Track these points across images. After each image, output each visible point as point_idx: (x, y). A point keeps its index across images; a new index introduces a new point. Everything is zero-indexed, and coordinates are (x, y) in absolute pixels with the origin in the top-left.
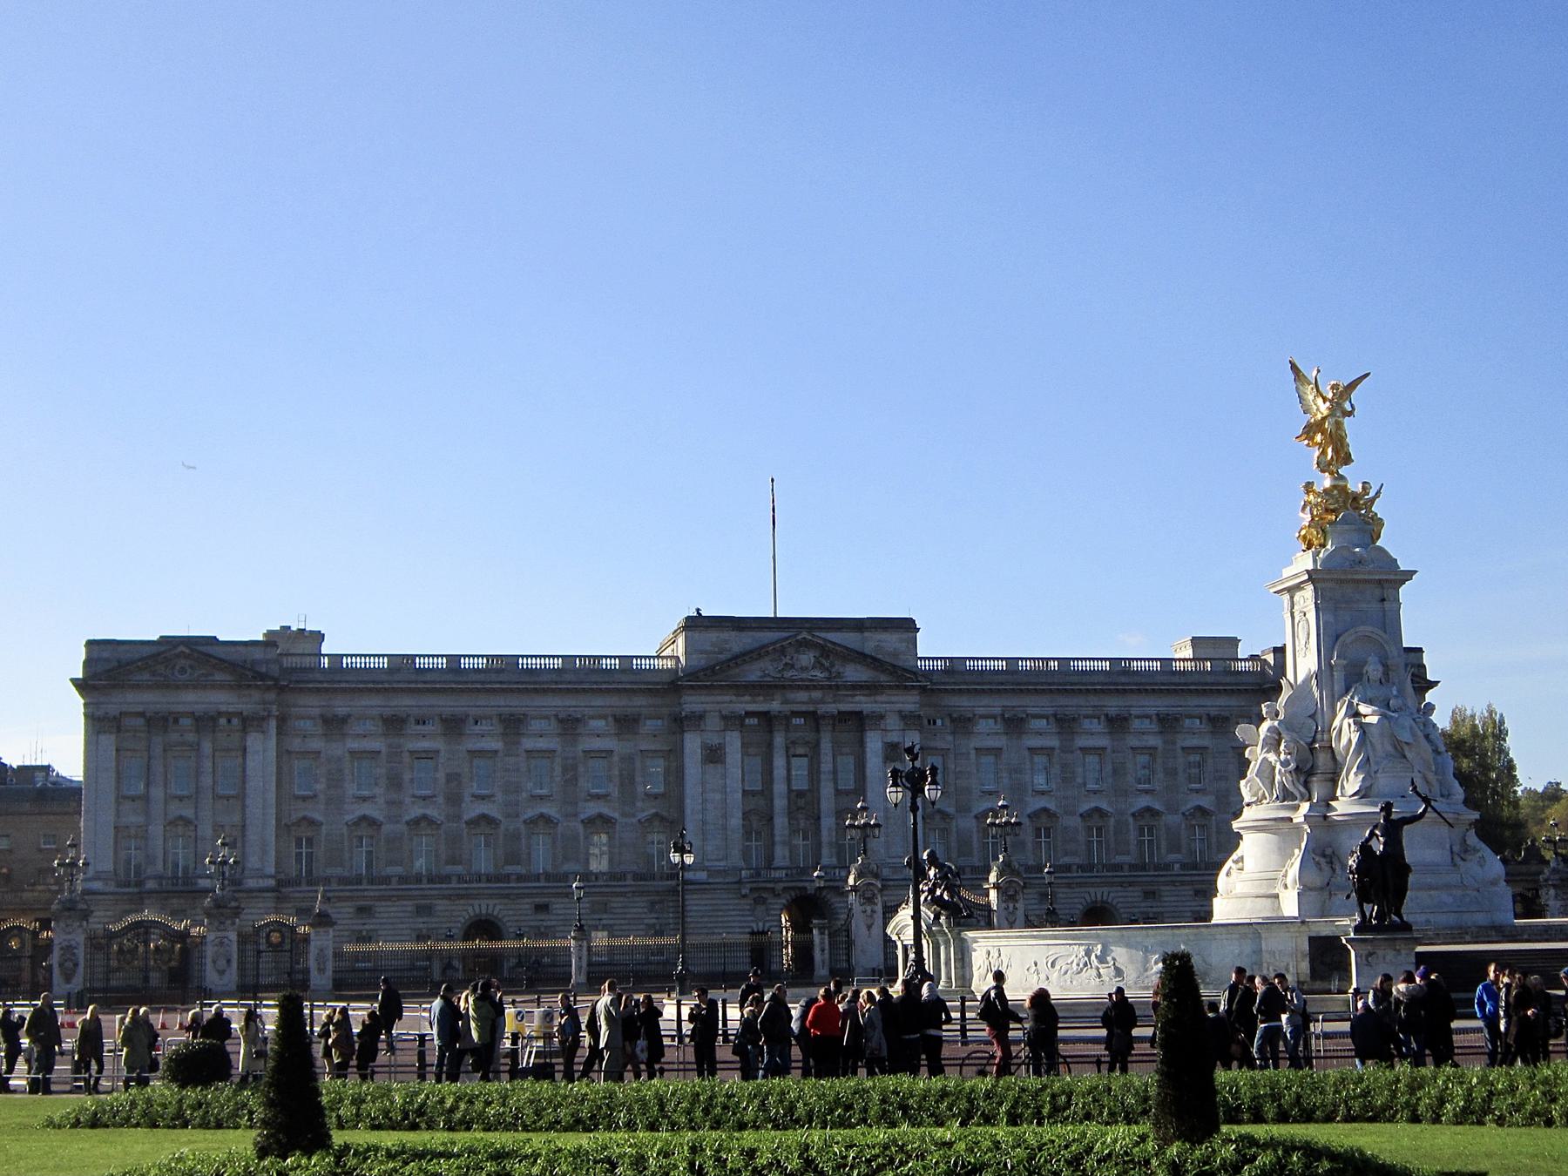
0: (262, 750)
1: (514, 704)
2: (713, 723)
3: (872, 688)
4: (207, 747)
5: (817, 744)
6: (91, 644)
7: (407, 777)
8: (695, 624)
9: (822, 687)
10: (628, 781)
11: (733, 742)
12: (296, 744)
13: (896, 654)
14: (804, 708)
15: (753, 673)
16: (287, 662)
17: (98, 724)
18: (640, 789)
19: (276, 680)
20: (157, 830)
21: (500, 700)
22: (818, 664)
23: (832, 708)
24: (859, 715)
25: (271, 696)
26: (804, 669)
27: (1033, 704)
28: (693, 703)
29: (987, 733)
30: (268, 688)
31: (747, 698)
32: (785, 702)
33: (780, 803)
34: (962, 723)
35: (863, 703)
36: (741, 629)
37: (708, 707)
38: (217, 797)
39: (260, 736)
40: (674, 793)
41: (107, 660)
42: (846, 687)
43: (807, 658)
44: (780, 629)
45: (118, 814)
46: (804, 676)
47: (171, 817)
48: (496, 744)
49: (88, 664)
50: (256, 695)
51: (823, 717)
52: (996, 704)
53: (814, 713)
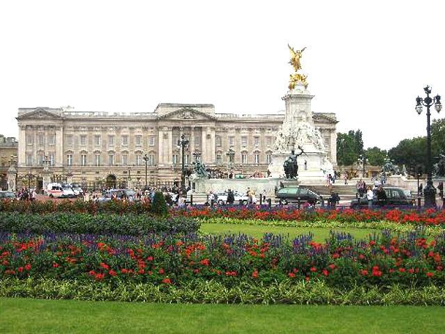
0: (59, 135)
2: (166, 129)
4: (46, 134)
7: (93, 141)
10: (145, 143)
11: (170, 133)
12: (68, 133)
15: (175, 118)
17: (22, 128)
18: (149, 145)
27: (242, 126)
28: (161, 124)
29: (232, 133)
30: (60, 120)
34: (225, 130)
35: (202, 125)
36: (173, 107)
40: (157, 146)
43: (188, 113)
48: (113, 133)
52: (233, 125)
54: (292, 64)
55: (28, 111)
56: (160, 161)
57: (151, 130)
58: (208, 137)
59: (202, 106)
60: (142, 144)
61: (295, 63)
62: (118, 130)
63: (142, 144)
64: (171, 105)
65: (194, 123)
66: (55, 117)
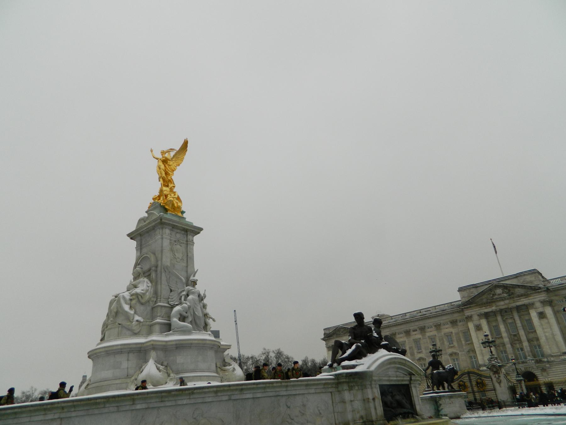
1: (421, 324)
2: (475, 318)
3: (526, 295)
5: (513, 318)
6: (324, 329)
8: (461, 290)
9: (508, 299)
10: (459, 341)
11: (484, 323)
13: (531, 282)
14: (504, 307)
18: (463, 342)
21: (417, 323)
23: (514, 305)
24: (524, 305)
26: (499, 295)
28: (468, 313)
32: (497, 306)
33: (506, 340)
35: (524, 301)
36: (476, 287)
37: (472, 313)
42: (516, 297)
43: (499, 291)
49: (324, 334)
51: (511, 309)
56: (481, 362)
57: (461, 323)
58: (542, 315)
59: (517, 276)
60: (455, 344)
62: (423, 329)
63: (455, 344)
64: (475, 286)
65: (511, 301)
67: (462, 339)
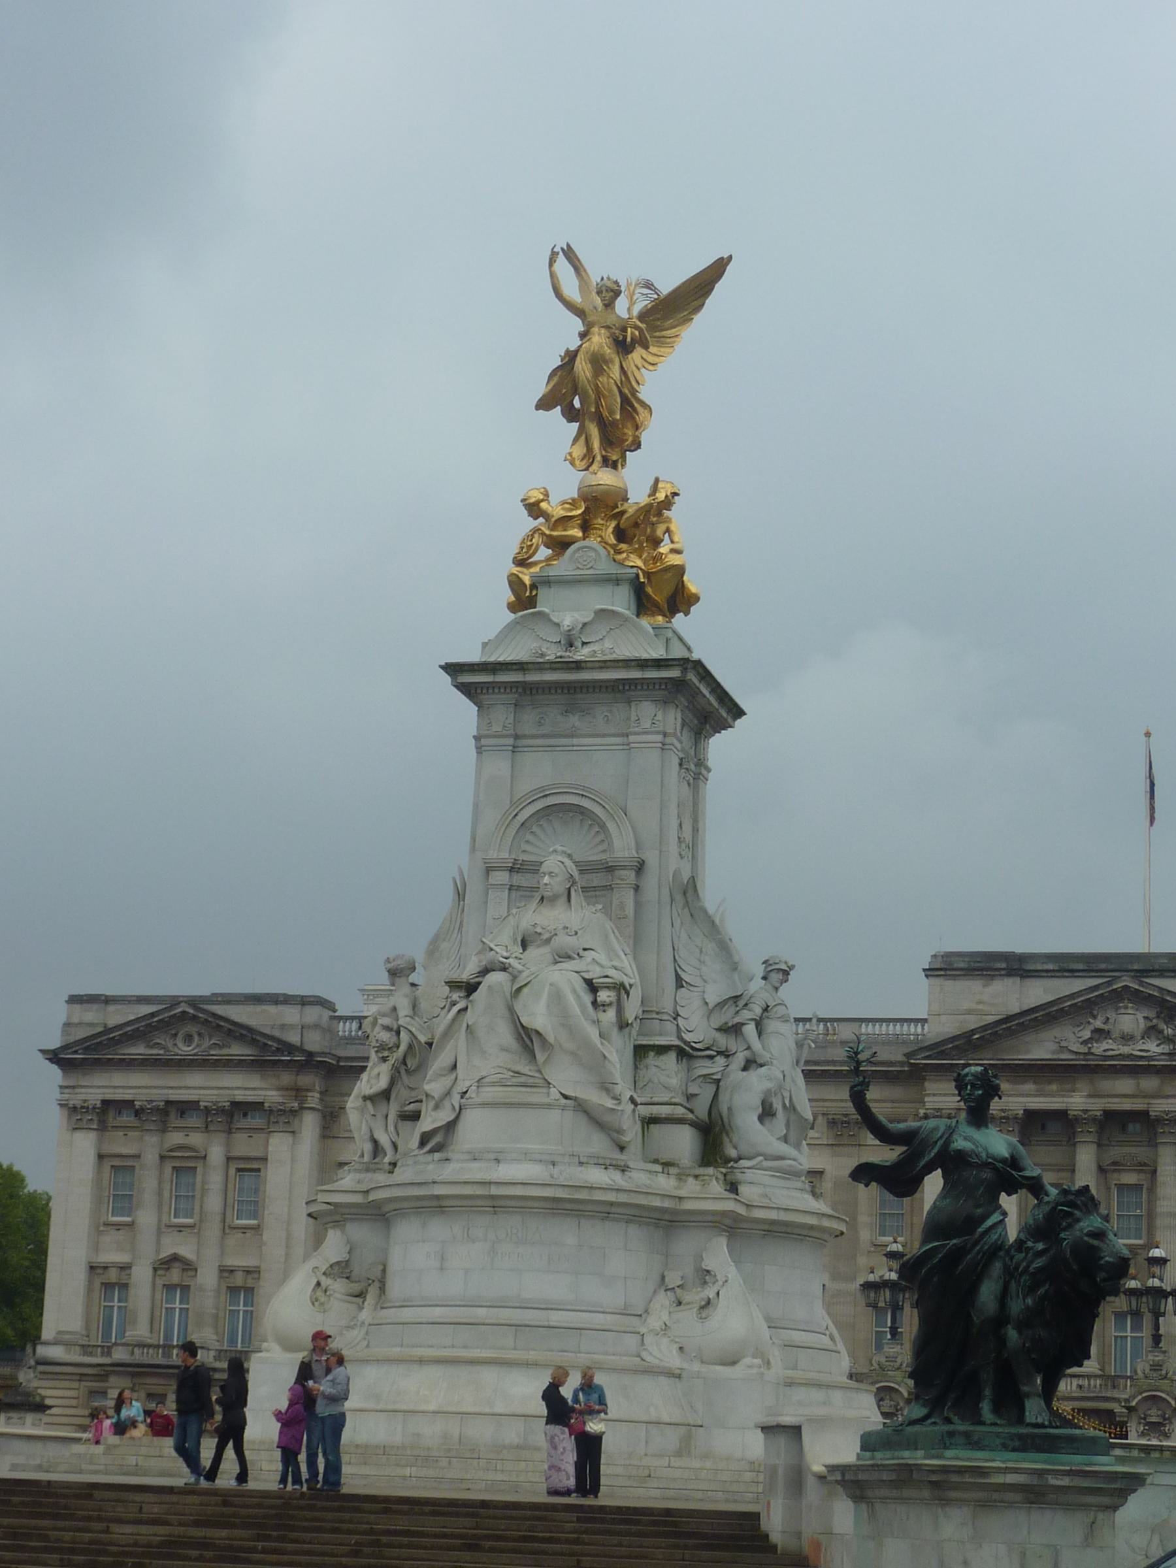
4: (216, 1153)
6: (74, 1000)
14: (1127, 1105)
16: (344, 1029)
18: (865, 1235)
19: (310, 1054)
20: (142, 1274)
22: (1152, 1031)
25: (305, 1080)
26: (1127, 1038)
31: (1029, 1087)
38: (227, 1228)
39: (288, 1138)
41: (91, 1025)
43: (1131, 1020)
44: (1089, 972)
45: (96, 1247)
46: (1125, 1050)
47: (164, 1255)
49: (67, 1025)
50: (287, 1078)
51: (1159, 1120)
53: (1142, 1116)
54: (571, 415)
55: (116, 1016)
61: (596, 404)
64: (1017, 966)
66: (268, 1053)
67: (863, 1219)
